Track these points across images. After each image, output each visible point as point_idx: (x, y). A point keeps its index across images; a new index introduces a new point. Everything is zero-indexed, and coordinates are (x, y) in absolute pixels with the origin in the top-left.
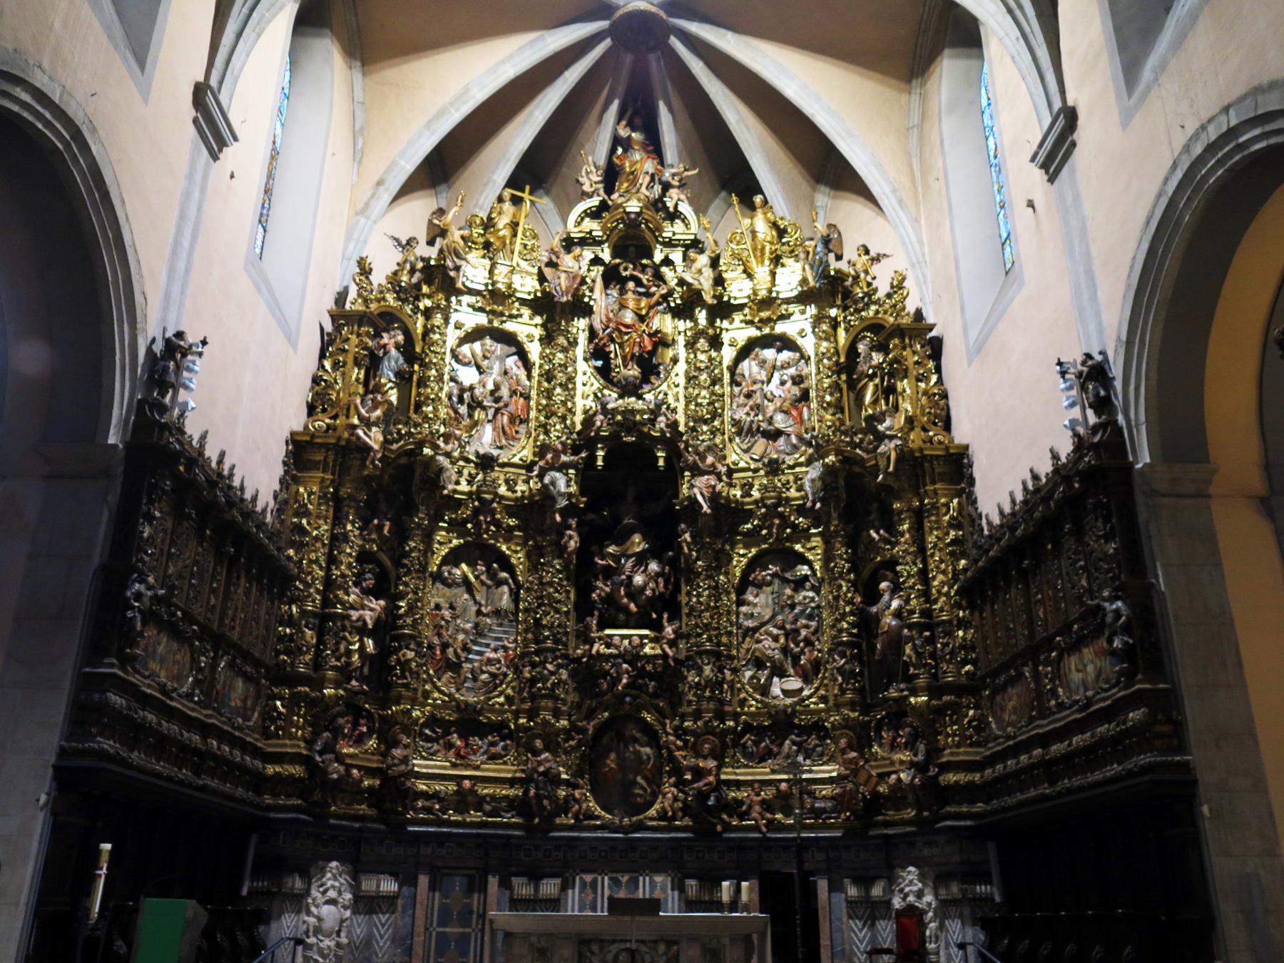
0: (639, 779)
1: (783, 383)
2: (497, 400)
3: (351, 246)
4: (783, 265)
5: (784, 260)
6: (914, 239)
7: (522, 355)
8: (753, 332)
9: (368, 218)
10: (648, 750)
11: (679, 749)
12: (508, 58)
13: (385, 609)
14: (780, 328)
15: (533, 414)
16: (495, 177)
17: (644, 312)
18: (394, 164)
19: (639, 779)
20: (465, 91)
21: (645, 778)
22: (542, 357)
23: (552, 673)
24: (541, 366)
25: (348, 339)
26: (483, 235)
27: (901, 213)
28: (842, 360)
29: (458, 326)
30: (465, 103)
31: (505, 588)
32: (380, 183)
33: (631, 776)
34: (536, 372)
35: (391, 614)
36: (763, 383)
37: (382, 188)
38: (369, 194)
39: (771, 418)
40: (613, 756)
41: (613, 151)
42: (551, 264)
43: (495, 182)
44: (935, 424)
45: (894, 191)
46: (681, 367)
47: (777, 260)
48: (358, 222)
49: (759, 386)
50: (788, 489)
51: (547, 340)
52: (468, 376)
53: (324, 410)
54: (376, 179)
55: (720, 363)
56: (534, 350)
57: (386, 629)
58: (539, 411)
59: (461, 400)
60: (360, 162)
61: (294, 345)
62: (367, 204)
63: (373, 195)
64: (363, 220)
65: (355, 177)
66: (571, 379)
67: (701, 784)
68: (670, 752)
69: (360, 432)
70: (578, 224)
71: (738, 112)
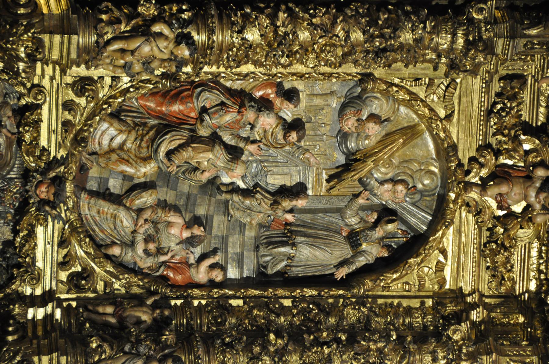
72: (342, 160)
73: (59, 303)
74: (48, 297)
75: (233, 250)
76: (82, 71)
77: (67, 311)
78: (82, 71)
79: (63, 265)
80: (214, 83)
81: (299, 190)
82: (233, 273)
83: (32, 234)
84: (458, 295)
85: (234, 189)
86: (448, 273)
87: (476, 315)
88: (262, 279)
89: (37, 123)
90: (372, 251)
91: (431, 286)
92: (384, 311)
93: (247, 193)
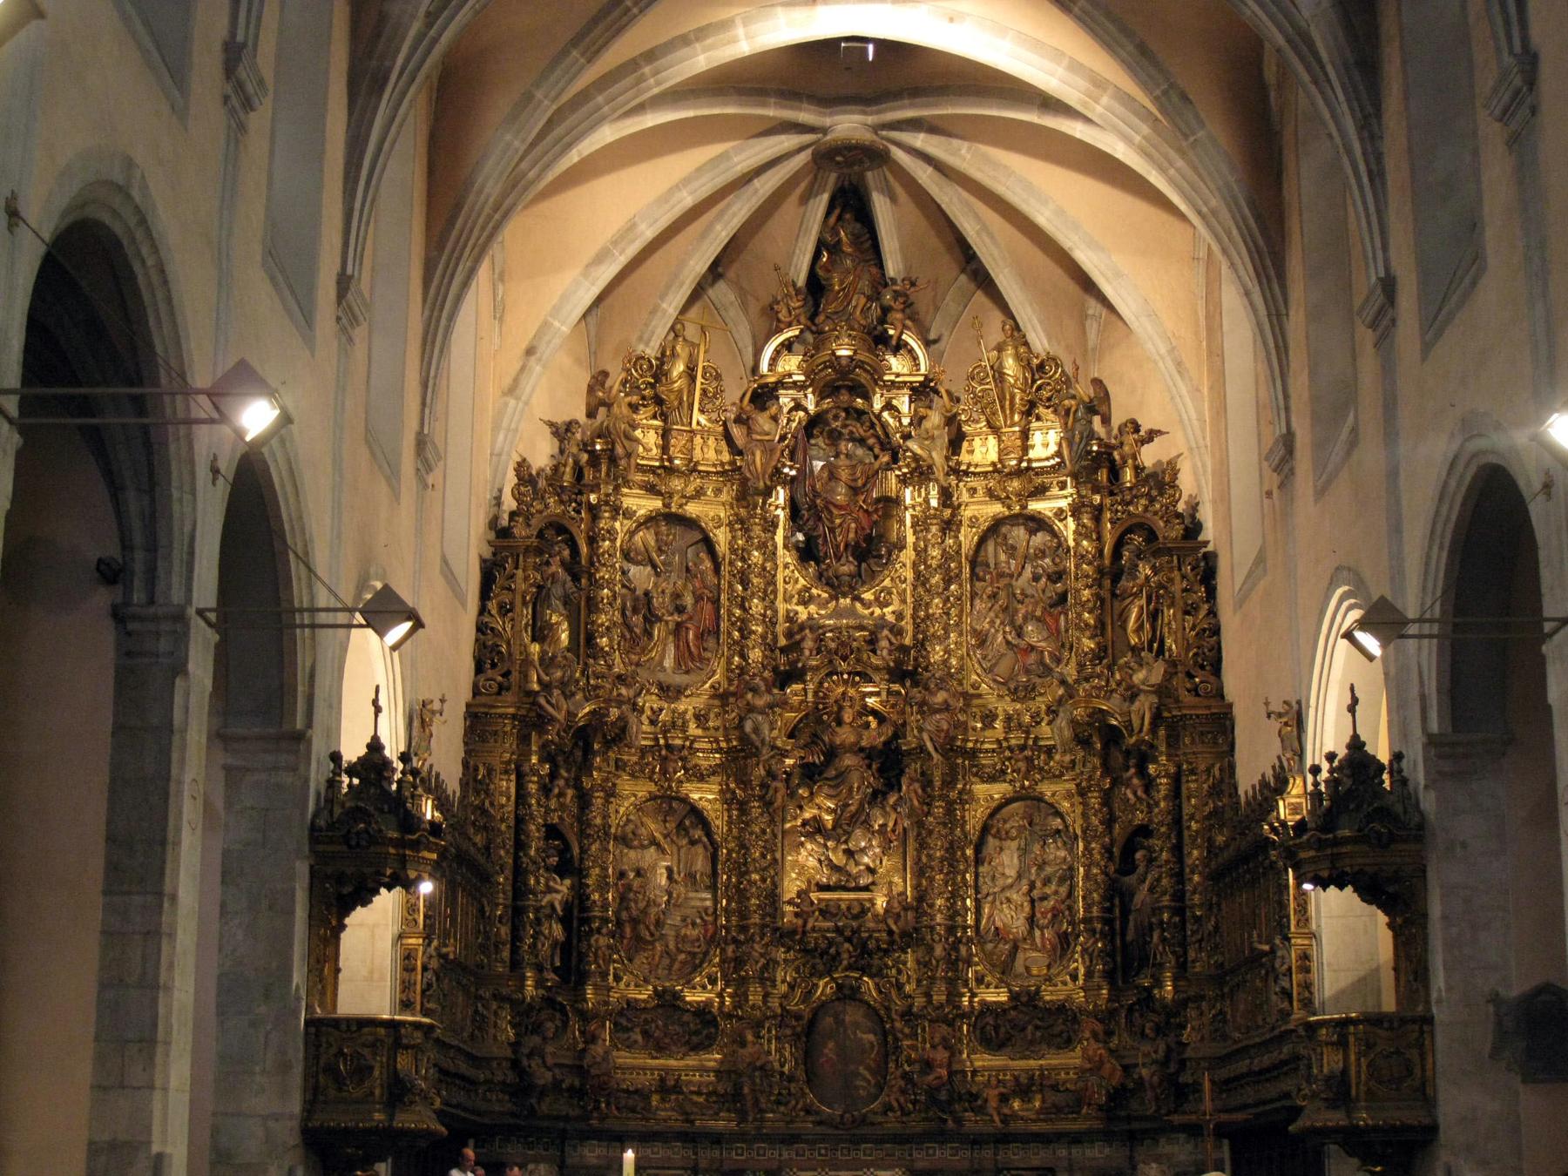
0: (861, 1070)
1: (1036, 578)
2: (680, 610)
3: (501, 437)
4: (1038, 418)
5: (1041, 410)
6: (1194, 416)
7: (708, 544)
8: (997, 509)
9: (518, 399)
10: (871, 1037)
11: (907, 1036)
12: (686, 181)
13: (572, 888)
14: (1035, 506)
15: (724, 625)
16: (664, 305)
17: (860, 483)
18: (546, 325)
19: (861, 1070)
20: (631, 227)
21: (868, 1068)
22: (733, 551)
23: (762, 955)
24: (731, 563)
25: (512, 576)
26: (653, 386)
27: (1177, 377)
28: (1107, 562)
29: (628, 514)
30: (633, 241)
31: (699, 849)
32: (530, 351)
33: (852, 1067)
34: (725, 569)
35: (580, 897)
36: (1011, 576)
37: (533, 358)
38: (518, 366)
39: (1021, 627)
40: (831, 1045)
41: (817, 255)
42: (738, 420)
43: (665, 312)
44: (1202, 667)
45: (1172, 350)
46: (908, 555)
47: (1030, 410)
48: (506, 404)
49: (1005, 581)
50: (1038, 723)
51: (740, 524)
52: (640, 575)
53: (494, 665)
54: (524, 346)
55: (958, 552)
56: (721, 537)
57: (576, 914)
58: (733, 624)
59: (635, 611)
60: (501, 320)
61: (464, 605)
62: (516, 380)
63: (523, 369)
64: (512, 402)
65: (497, 340)
66: (772, 582)
67: (931, 1077)
68: (896, 1039)
69: (542, 701)
70: (774, 361)
71: (978, 218)
72: (653, 849)
73: (723, 990)
74: (720, 995)
75: (698, 904)
76: (611, 978)
77: (727, 986)
78: (611, 978)
79: (704, 987)
80: (617, 913)
81: (669, 870)
82: (708, 903)
83: (690, 1003)
84: (721, 791)
85: (668, 901)
86: (711, 797)
87: (732, 786)
88: (713, 888)
89: (636, 1000)
90: (698, 833)
91: (718, 806)
92: (730, 830)
93: (670, 894)
